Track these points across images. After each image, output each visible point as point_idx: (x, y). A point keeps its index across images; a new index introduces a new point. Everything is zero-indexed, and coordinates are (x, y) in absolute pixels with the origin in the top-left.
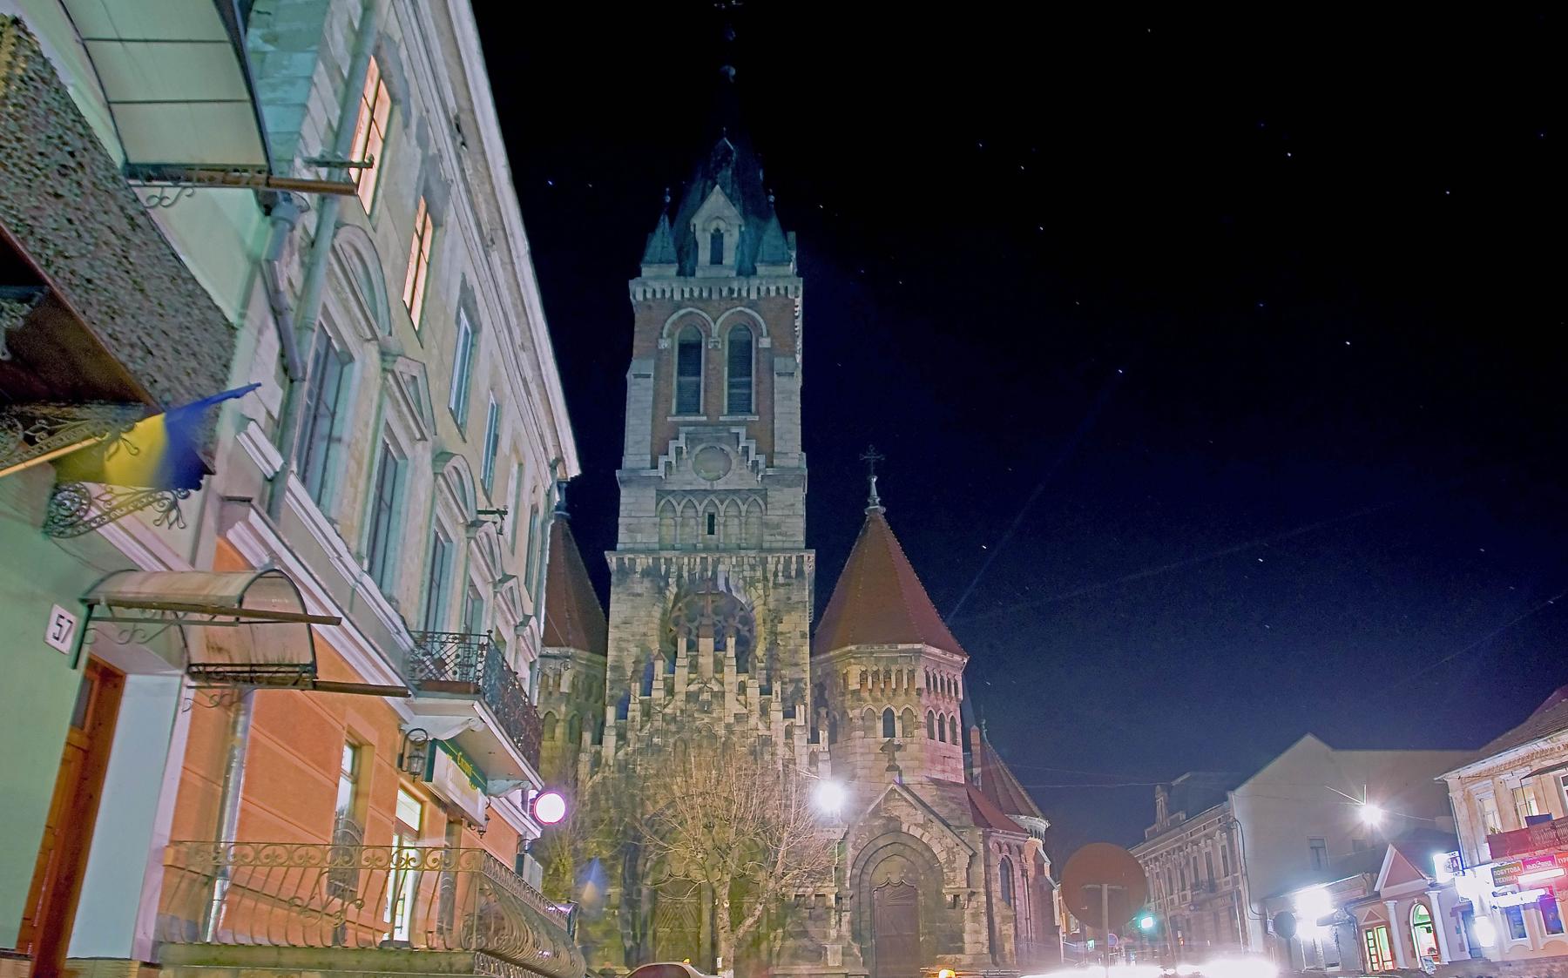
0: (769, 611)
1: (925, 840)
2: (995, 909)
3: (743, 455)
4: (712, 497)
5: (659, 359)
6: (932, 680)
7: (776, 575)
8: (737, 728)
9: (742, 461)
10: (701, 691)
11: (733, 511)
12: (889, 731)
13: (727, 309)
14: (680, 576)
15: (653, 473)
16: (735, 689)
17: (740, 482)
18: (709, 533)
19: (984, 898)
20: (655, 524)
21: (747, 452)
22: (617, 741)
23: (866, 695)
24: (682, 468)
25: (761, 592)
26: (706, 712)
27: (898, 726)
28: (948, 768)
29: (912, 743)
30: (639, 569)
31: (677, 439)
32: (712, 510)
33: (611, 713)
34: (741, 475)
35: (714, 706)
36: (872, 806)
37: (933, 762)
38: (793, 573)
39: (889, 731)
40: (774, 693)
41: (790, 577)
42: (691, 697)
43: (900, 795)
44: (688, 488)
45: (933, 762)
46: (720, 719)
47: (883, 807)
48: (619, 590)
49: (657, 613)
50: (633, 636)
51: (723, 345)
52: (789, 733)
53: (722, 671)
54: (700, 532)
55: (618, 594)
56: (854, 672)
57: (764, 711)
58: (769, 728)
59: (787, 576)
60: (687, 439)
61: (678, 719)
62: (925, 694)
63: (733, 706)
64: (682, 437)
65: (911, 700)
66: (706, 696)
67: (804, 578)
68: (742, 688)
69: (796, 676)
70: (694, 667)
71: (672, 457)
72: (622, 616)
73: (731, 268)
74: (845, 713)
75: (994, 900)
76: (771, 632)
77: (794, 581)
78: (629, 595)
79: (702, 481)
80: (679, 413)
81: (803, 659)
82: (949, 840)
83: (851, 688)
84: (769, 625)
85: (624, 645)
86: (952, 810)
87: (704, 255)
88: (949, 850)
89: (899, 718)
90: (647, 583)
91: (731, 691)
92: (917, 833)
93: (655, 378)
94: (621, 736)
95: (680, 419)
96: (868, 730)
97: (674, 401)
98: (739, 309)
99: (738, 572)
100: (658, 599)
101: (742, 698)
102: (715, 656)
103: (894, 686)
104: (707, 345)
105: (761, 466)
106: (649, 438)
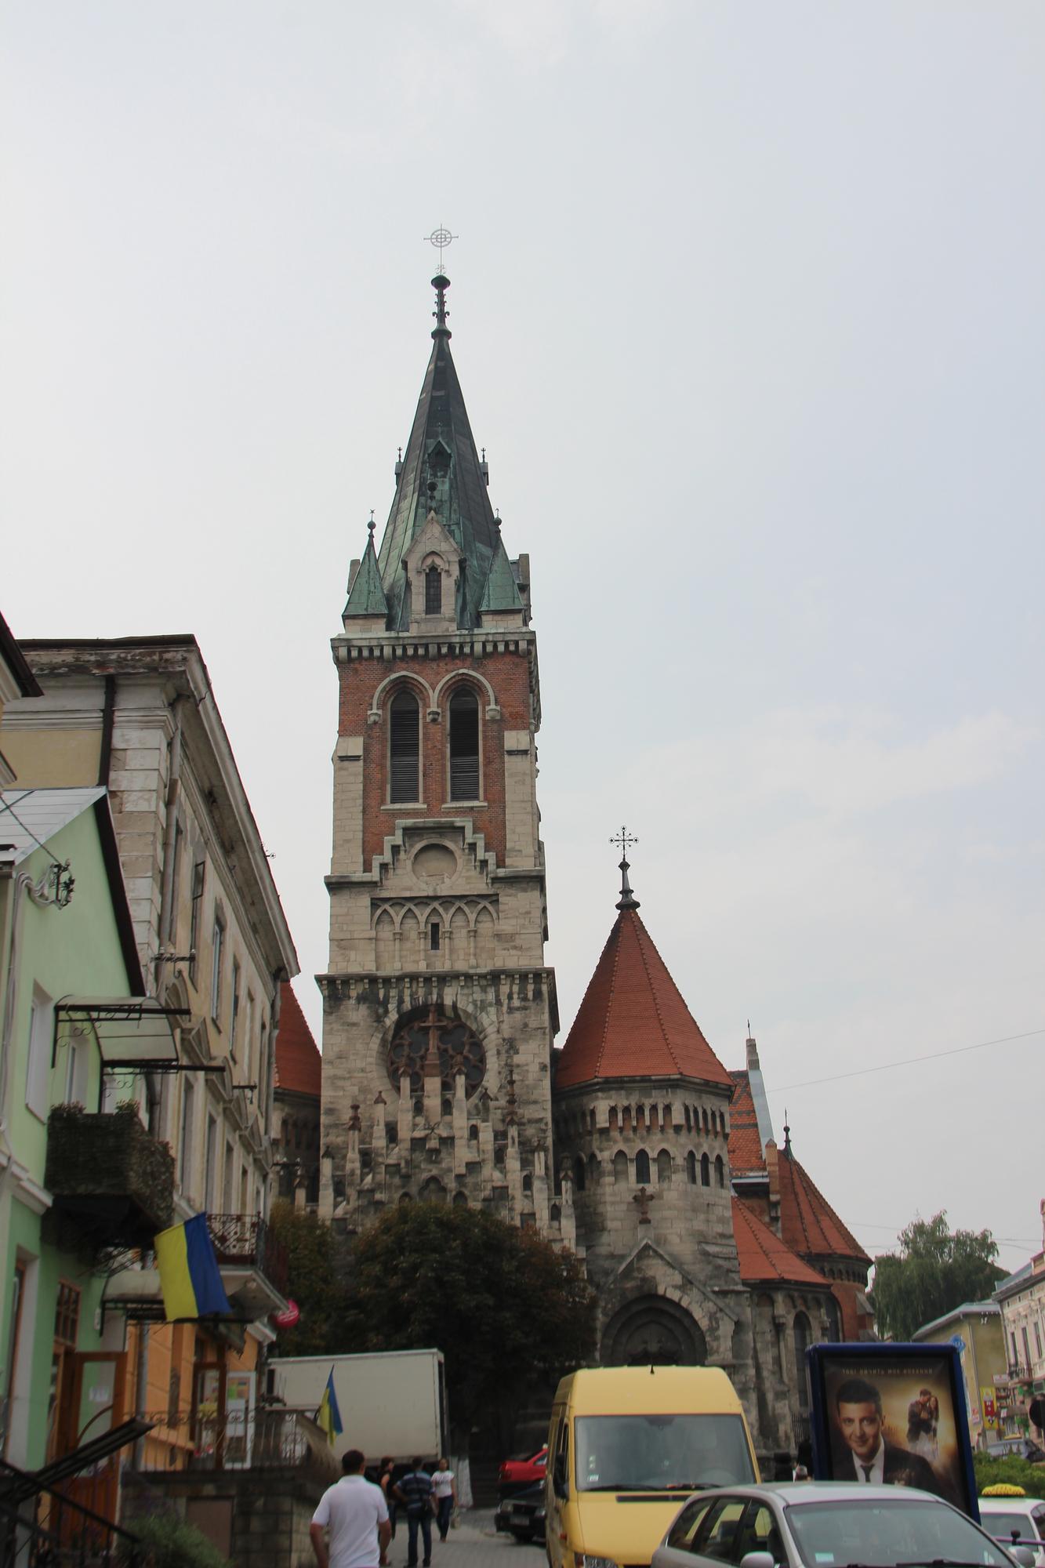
0: (504, 1040)
1: (684, 1304)
2: (767, 1384)
3: (469, 855)
4: (436, 904)
5: (369, 736)
6: (692, 1114)
7: (510, 997)
8: (469, 1180)
9: (470, 860)
10: (424, 1140)
11: (459, 921)
12: (643, 1176)
13: (448, 672)
14: (401, 1001)
15: (367, 877)
16: (466, 1133)
17: (468, 887)
18: (432, 949)
19: (752, 1372)
20: (370, 939)
21: (475, 850)
22: (335, 1198)
23: (615, 1134)
24: (399, 871)
25: (494, 1018)
26: (431, 1162)
27: (653, 1169)
28: (713, 1218)
29: (669, 1189)
30: (353, 993)
32: (435, 920)
33: (326, 1167)
34: (468, 878)
35: (443, 1155)
36: (623, 1266)
37: (694, 1210)
38: (530, 995)
39: (643, 1176)
40: (510, 1141)
42: (417, 1144)
43: (655, 1252)
44: (407, 894)
45: (694, 1210)
46: (450, 1170)
47: (635, 1266)
48: (332, 1018)
49: (375, 1043)
50: (349, 1072)
51: (444, 716)
52: (527, 1183)
53: (450, 1113)
54: (422, 947)
55: (331, 1024)
56: (602, 1106)
57: (500, 1156)
59: (525, 999)
60: (404, 835)
61: (404, 1171)
62: (684, 1132)
63: (463, 1154)
64: (399, 833)
66: (433, 1144)
67: (542, 1000)
68: (474, 1132)
69: (537, 1116)
70: (418, 1108)
71: (387, 857)
72: (336, 1049)
74: (593, 1156)
75: (765, 1374)
76: (506, 1065)
77: (530, 1004)
78: (343, 1024)
79: (424, 886)
80: (393, 801)
81: (543, 1096)
82: (711, 1304)
83: (598, 1126)
84: (504, 1056)
85: (340, 1083)
86: (718, 1267)
87: (418, 602)
88: (712, 1317)
89: (654, 1160)
91: (461, 1138)
92: (674, 1295)
93: (365, 761)
94: (339, 1190)
95: (397, 806)
96: (618, 1174)
97: (389, 787)
98: (462, 671)
100: (377, 1029)
101: (474, 1142)
102: (442, 1095)
103: (648, 1123)
104: (424, 717)
105: (491, 866)
106: (360, 835)
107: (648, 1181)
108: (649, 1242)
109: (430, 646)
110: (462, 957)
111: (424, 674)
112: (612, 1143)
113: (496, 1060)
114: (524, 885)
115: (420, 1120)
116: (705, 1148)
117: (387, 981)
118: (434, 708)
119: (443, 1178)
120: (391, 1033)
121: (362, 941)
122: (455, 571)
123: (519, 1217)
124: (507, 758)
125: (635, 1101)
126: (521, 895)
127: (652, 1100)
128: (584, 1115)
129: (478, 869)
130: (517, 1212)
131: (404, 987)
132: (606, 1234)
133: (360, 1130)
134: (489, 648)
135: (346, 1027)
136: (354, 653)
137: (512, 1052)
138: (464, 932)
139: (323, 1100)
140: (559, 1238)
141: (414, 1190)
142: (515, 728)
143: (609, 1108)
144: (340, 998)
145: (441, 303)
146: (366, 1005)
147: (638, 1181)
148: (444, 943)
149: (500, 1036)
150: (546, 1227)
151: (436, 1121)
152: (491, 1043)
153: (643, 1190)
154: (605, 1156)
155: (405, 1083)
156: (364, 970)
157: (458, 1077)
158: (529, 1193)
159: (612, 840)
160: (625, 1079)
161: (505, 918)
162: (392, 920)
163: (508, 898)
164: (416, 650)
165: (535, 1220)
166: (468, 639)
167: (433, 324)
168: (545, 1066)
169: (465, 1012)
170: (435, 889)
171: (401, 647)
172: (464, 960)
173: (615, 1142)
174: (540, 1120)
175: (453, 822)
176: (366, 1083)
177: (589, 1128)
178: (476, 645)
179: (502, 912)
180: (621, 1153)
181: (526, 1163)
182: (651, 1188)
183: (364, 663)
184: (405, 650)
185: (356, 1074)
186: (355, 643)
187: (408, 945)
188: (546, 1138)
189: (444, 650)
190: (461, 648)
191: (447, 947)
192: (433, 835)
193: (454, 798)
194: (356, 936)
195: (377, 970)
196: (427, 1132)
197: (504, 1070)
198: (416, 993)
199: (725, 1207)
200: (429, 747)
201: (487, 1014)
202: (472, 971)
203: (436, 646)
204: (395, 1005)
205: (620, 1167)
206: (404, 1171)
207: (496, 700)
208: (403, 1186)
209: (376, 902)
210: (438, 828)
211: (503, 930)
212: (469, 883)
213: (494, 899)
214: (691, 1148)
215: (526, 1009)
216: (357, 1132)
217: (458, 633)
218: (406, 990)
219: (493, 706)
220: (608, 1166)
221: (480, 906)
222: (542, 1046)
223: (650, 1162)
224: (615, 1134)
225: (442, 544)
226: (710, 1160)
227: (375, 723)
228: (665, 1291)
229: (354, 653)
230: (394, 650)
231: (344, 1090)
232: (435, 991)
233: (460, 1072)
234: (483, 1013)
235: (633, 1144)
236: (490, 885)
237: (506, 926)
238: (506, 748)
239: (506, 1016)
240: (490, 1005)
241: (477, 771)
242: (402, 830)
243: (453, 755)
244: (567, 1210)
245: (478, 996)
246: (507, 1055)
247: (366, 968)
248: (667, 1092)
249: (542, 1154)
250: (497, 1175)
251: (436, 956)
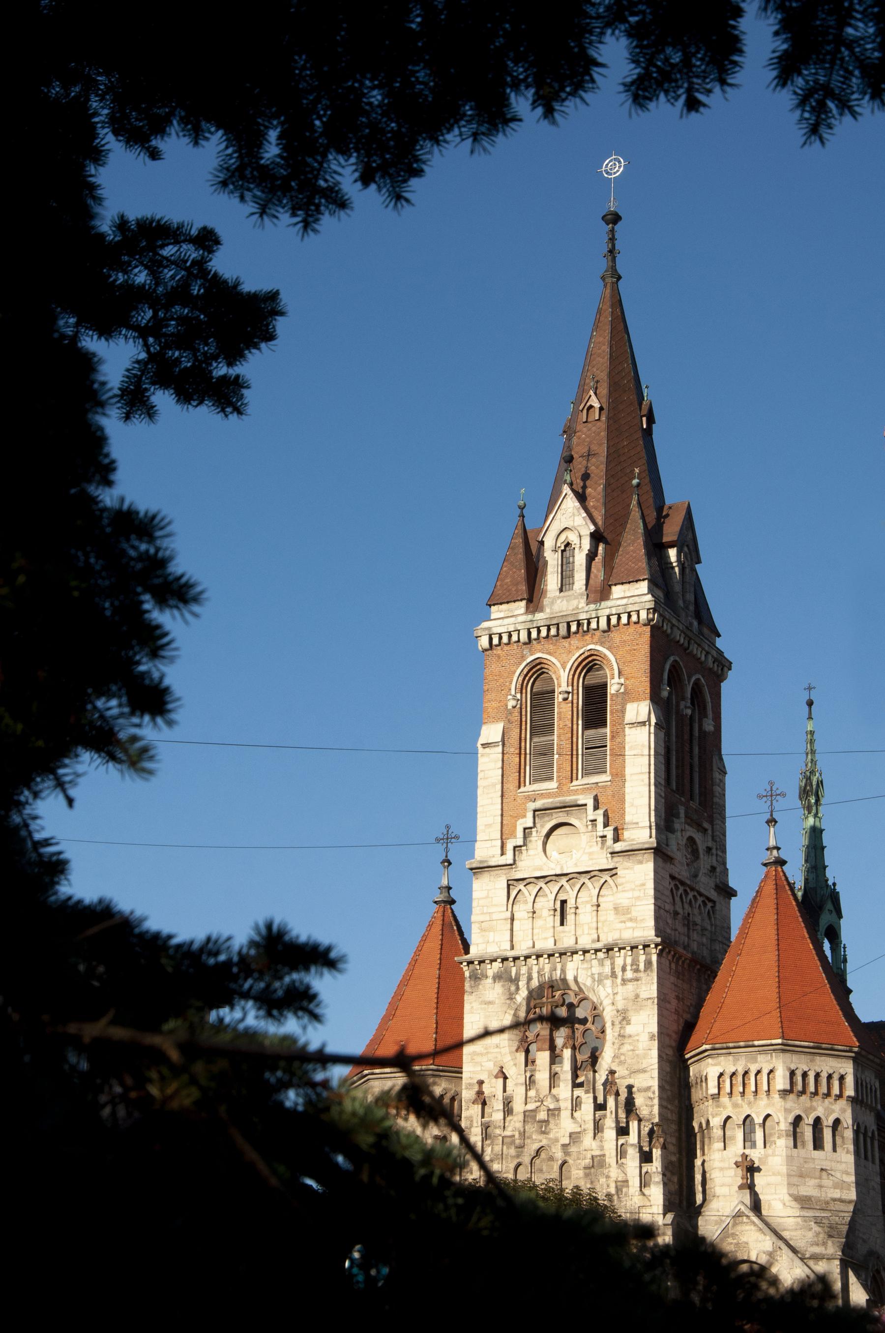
0: (618, 1011)
4: (563, 881)
6: (799, 1079)
7: (624, 969)
8: (573, 1149)
10: (535, 1111)
13: (578, 648)
14: (530, 979)
17: (591, 862)
24: (531, 852)
25: (609, 990)
26: (544, 1133)
27: (759, 1135)
29: (774, 1155)
30: (490, 973)
31: (525, 816)
32: (562, 897)
34: (590, 854)
35: (551, 1126)
38: (642, 966)
41: (637, 970)
42: (528, 1116)
43: (747, 1216)
45: (801, 1176)
47: (730, 1231)
50: (486, 1049)
53: (559, 1086)
54: (552, 924)
55: (471, 1003)
57: (598, 1128)
58: (602, 1148)
59: (637, 970)
61: (518, 1142)
64: (530, 815)
65: (773, 1105)
66: (542, 1115)
67: (652, 971)
69: (645, 1084)
70: (530, 1082)
73: (582, 594)
74: (708, 1122)
76: (622, 1036)
77: (641, 975)
79: (552, 865)
85: (478, 1059)
90: (499, 988)
91: (566, 1109)
93: (503, 745)
95: (536, 786)
99: (587, 969)
103: (753, 1089)
107: (754, 1145)
108: (743, 1208)
109: (560, 625)
110: (586, 932)
111: (557, 654)
112: (722, 1109)
113: (611, 1031)
114: (640, 858)
115: (532, 1093)
116: (820, 1112)
117: (516, 959)
118: (564, 687)
119: (550, 1147)
120: (523, 1009)
121: (499, 922)
122: (586, 544)
123: (613, 1185)
124: (627, 731)
125: (742, 1066)
126: (638, 867)
127: (757, 1065)
128: (702, 1081)
129: (600, 844)
130: (612, 1179)
131: (532, 965)
132: (715, 1199)
133: (484, 1103)
134: (614, 620)
135: (483, 1006)
136: (496, 641)
137: (624, 1022)
138: (589, 906)
139: (464, 1075)
140: (648, 1204)
141: (526, 1160)
142: (638, 700)
143: (718, 1074)
144: (479, 978)
145: (612, 239)
146: (501, 984)
147: (744, 1148)
148: (570, 918)
149: (614, 1008)
150: (637, 1193)
151: (545, 1094)
152: (608, 1014)
153: (745, 1156)
154: (716, 1122)
155: (521, 1056)
156: (501, 950)
157: (565, 1050)
158: (623, 1160)
159: (760, 797)
160: (731, 1045)
161: (623, 891)
162: (526, 900)
163: (626, 871)
164: (549, 630)
165: (628, 1186)
166: (594, 616)
167: (603, 265)
168: (653, 1036)
169: (584, 984)
170: (562, 868)
171: (536, 629)
172: (588, 934)
173: (725, 1107)
174: (648, 1089)
175: (577, 800)
176: (499, 1058)
177: (705, 1095)
178: (600, 618)
179: (620, 885)
180: (729, 1117)
181: (623, 1131)
182: (756, 1154)
183: (506, 648)
184: (539, 632)
185: (489, 1051)
186: (495, 630)
187: (538, 923)
188: (652, 1106)
189: (574, 628)
190: (589, 623)
191: (573, 922)
192: (561, 814)
193: (587, 773)
194: (495, 917)
195: (512, 948)
196: (539, 1104)
197: (616, 1041)
198: (543, 969)
199: (848, 1174)
200: (561, 726)
201: (604, 987)
202: (588, 947)
203: (565, 625)
204: (525, 982)
205: (728, 1133)
206: (518, 1142)
207: (620, 673)
208: (518, 1156)
209: (510, 882)
210: (565, 807)
211: (620, 904)
212: (592, 859)
213: (612, 872)
214: (798, 1112)
215: (638, 980)
216: (480, 1106)
217: (586, 609)
218: (534, 966)
219: (616, 680)
220: (717, 1132)
221: (602, 881)
222: (651, 1016)
223: (757, 1127)
224: (725, 1099)
225: (576, 518)
226: (825, 1123)
227: (514, 707)
228: (757, 1258)
229: (496, 641)
230: (529, 633)
231: (482, 1066)
232: (559, 966)
233: (565, 1046)
234: (600, 986)
235: (741, 1109)
236: (610, 859)
237: (623, 898)
238: (626, 722)
239: (620, 989)
240: (607, 978)
241: (606, 746)
242: (532, 812)
243: (586, 727)
244: (658, 1178)
245: (596, 970)
246: (620, 1026)
247: (502, 948)
248: (772, 1056)
249: (636, 1123)
250: (594, 1145)
251: (564, 932)
